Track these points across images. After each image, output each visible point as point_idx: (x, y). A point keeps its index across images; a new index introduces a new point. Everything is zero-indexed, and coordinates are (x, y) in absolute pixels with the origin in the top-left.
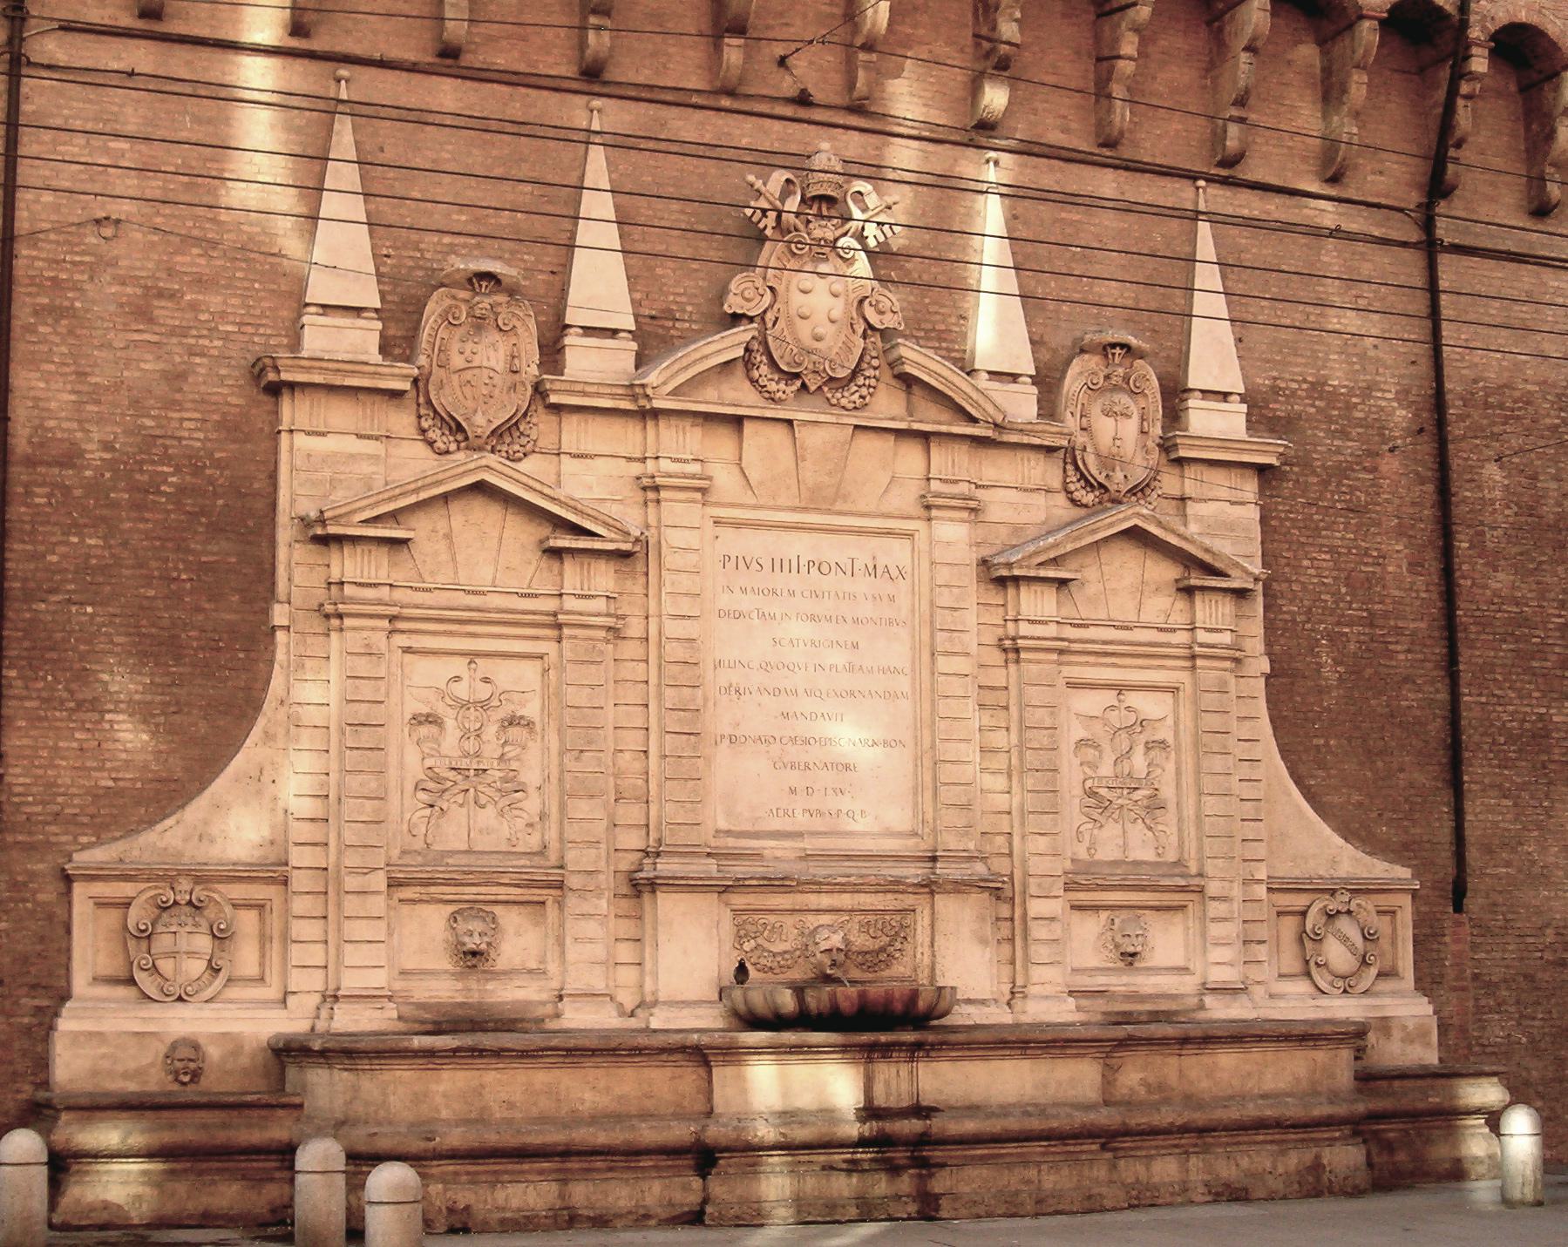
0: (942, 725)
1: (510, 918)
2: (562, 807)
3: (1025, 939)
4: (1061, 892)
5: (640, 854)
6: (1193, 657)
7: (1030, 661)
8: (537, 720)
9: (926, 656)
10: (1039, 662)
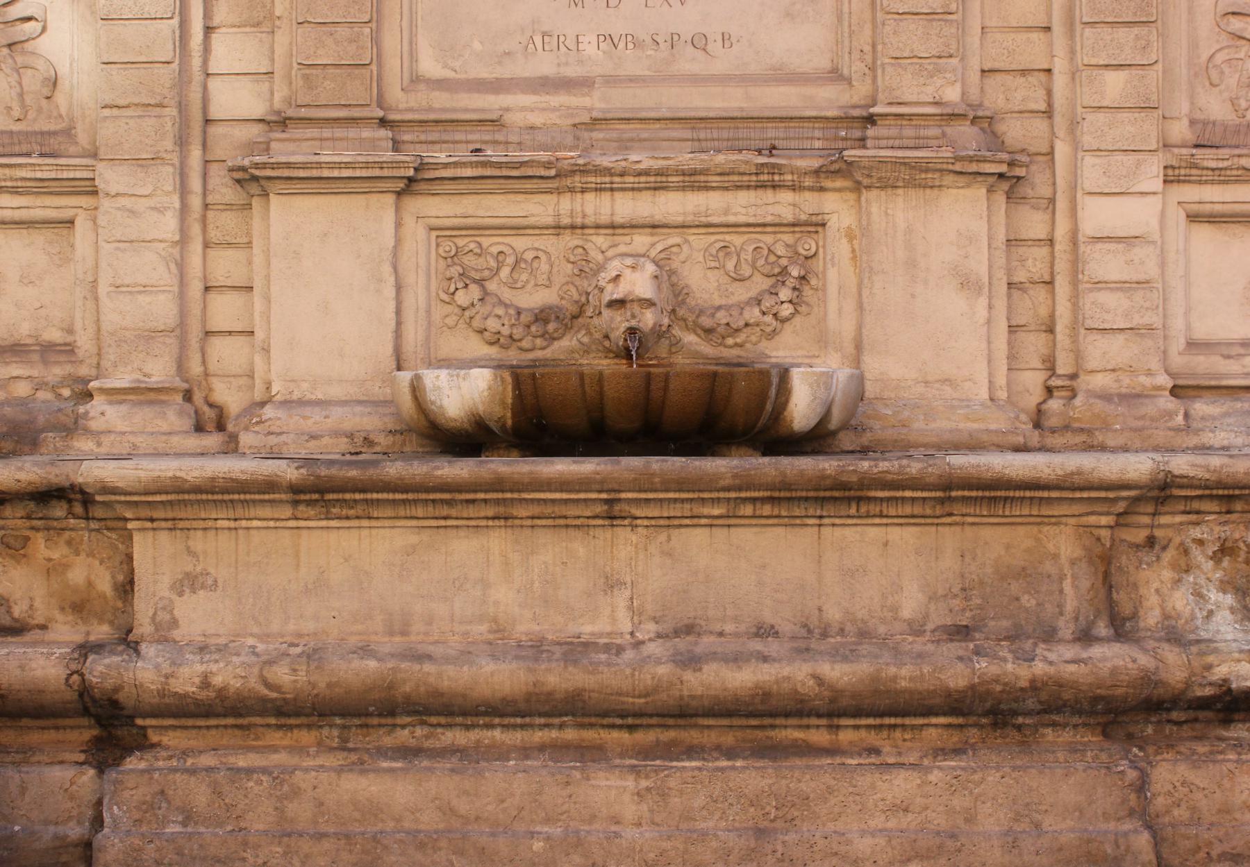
3: (1075, 283)
4: (1158, 185)
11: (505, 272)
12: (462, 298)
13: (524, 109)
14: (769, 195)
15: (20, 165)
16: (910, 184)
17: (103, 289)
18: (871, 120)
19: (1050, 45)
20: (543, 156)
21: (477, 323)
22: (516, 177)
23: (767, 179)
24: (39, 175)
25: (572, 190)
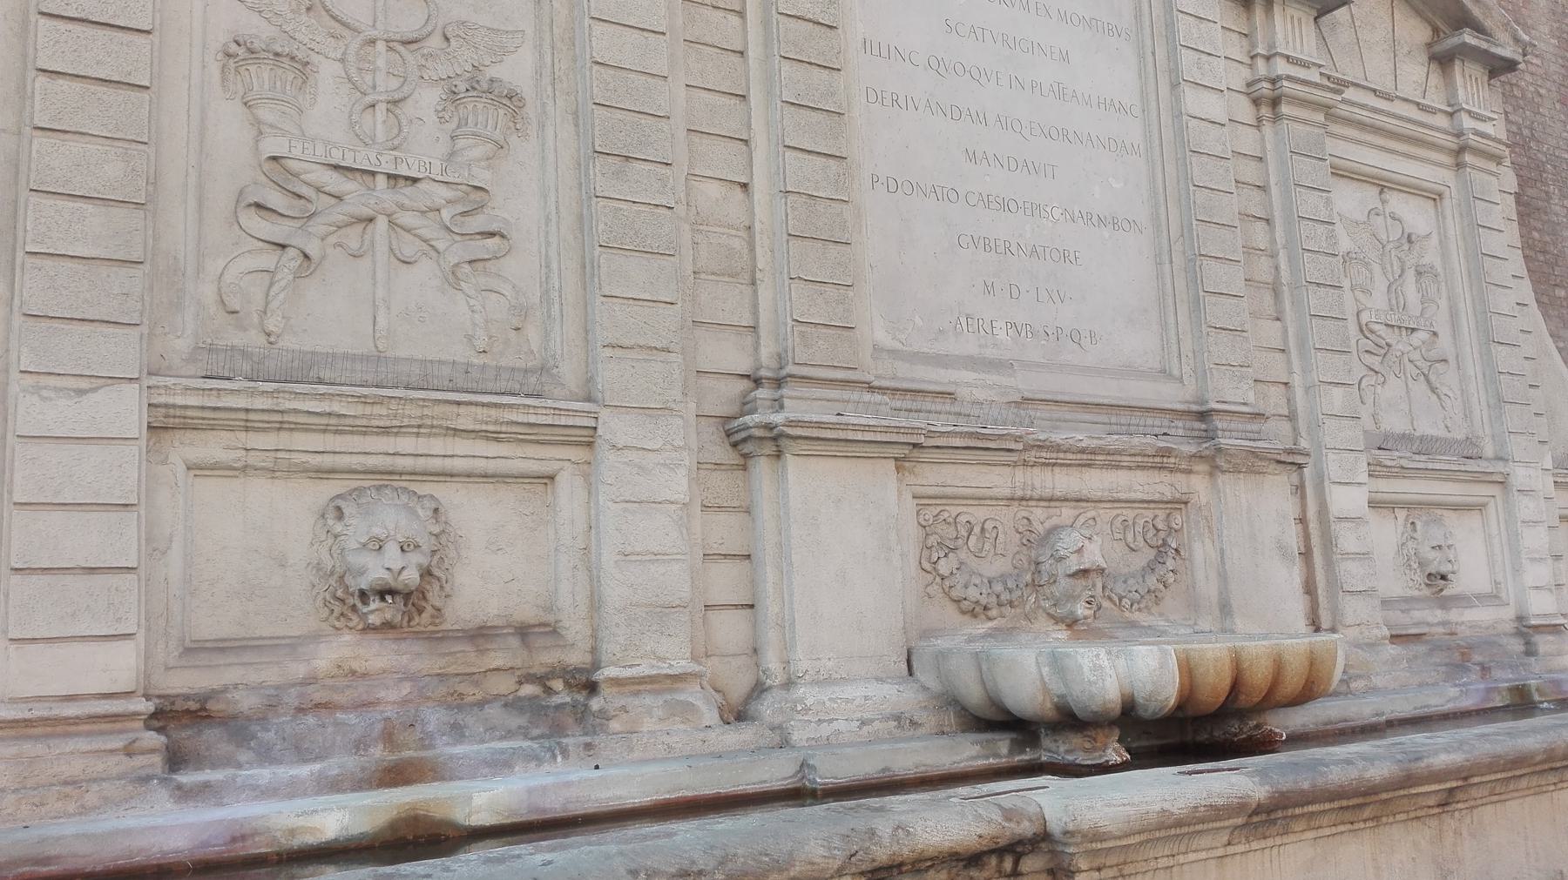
0: (1201, 196)
1: (476, 514)
2: (587, 270)
4: (1364, 477)
5: (745, 384)
6: (1461, 150)
7: (1295, 119)
8: (526, 89)
9: (1164, 89)
10: (1305, 122)
11: (973, 539)
12: (943, 567)
13: (968, 385)
14: (1156, 476)
15: (511, 406)
16: (1252, 471)
17: (608, 558)
18: (1203, 416)
19: (1289, 362)
20: (1013, 430)
21: (954, 594)
22: (980, 446)
23: (1160, 461)
24: (532, 419)
25: (1025, 464)
